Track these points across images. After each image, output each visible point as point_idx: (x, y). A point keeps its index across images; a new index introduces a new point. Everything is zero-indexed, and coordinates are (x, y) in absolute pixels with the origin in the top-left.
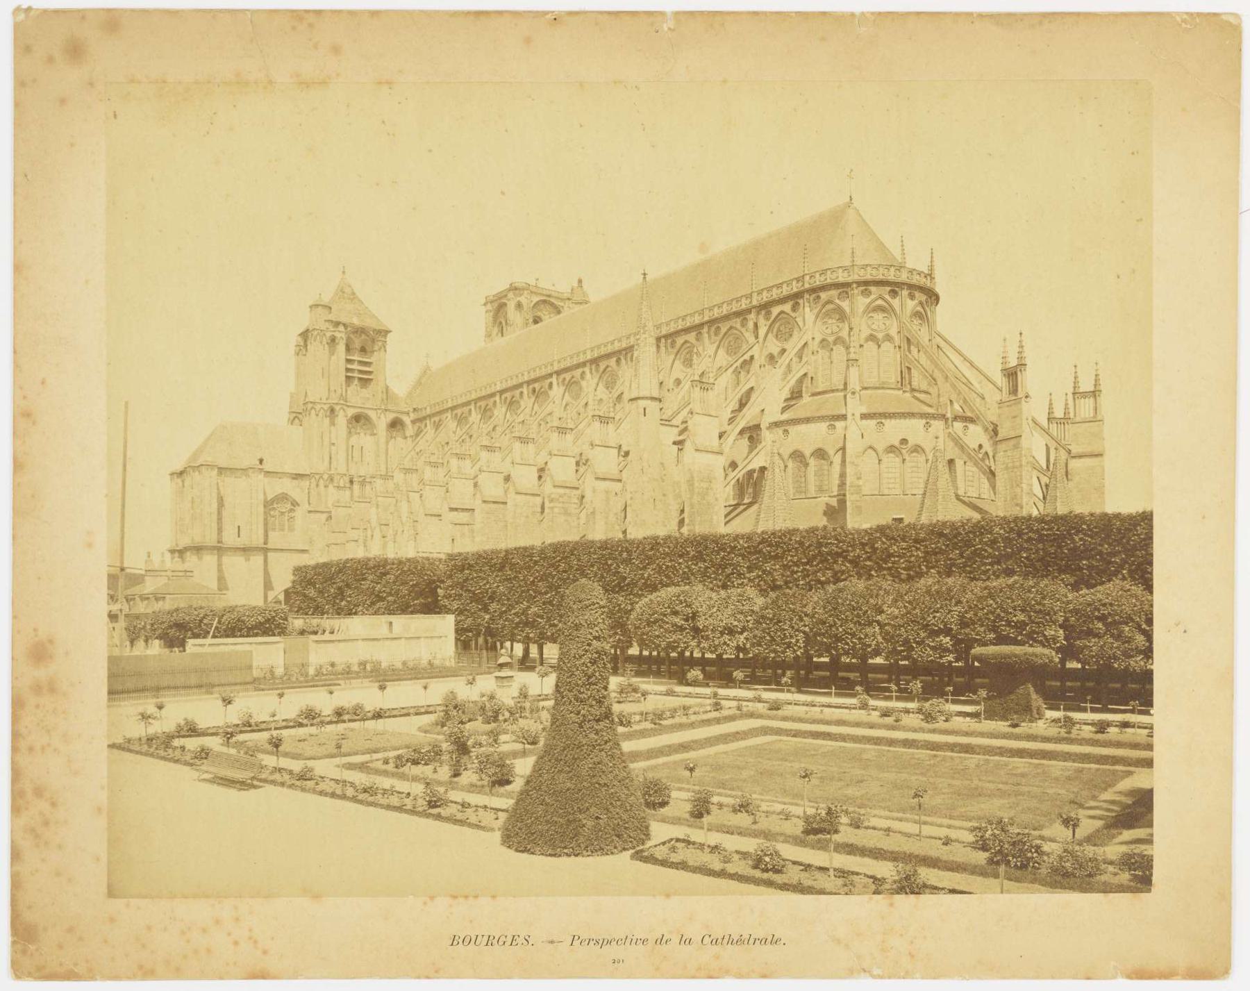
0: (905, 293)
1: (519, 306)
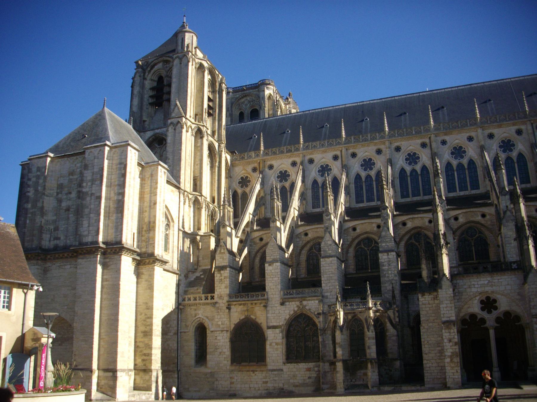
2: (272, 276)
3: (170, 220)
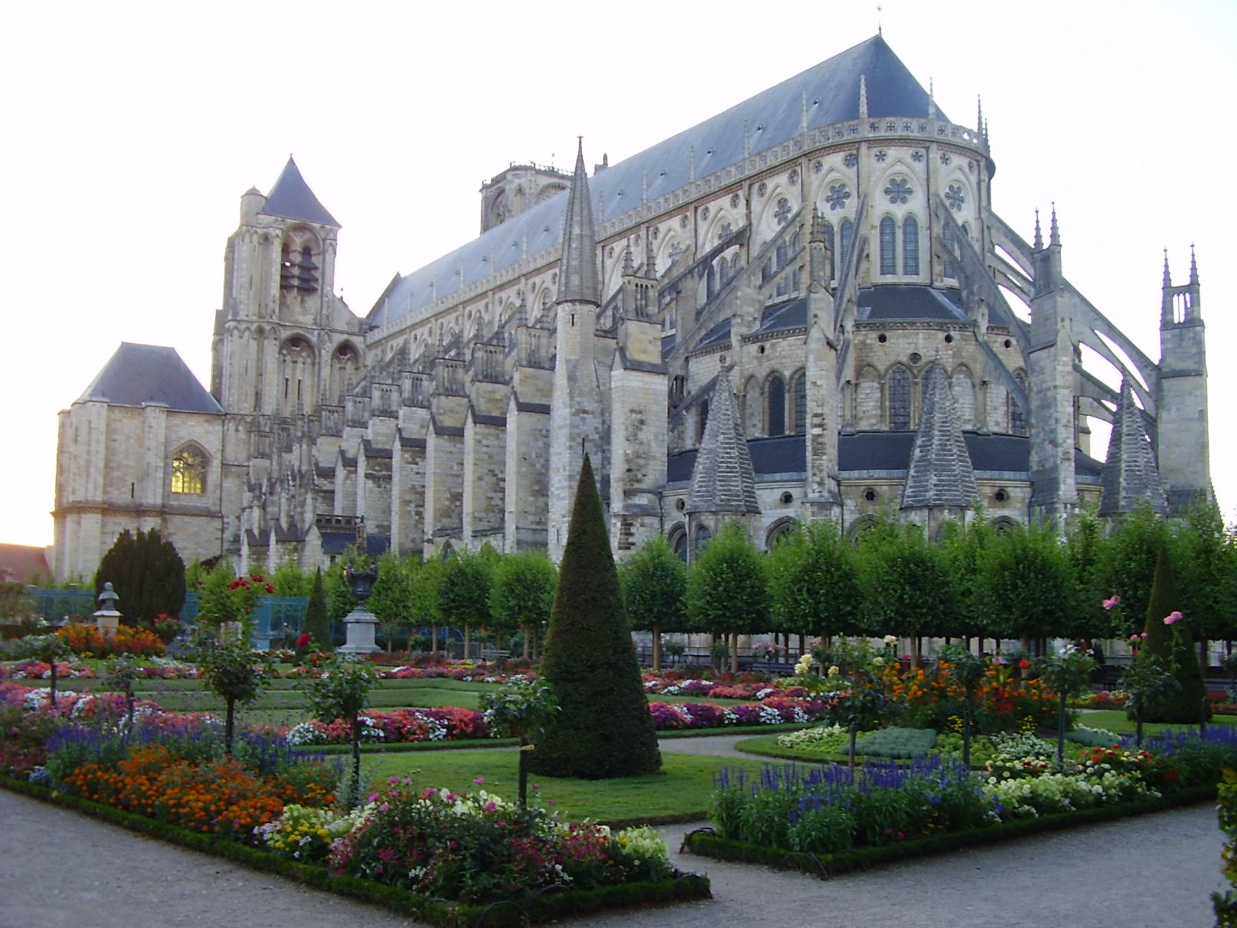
0: (935, 154)
1: (520, 190)
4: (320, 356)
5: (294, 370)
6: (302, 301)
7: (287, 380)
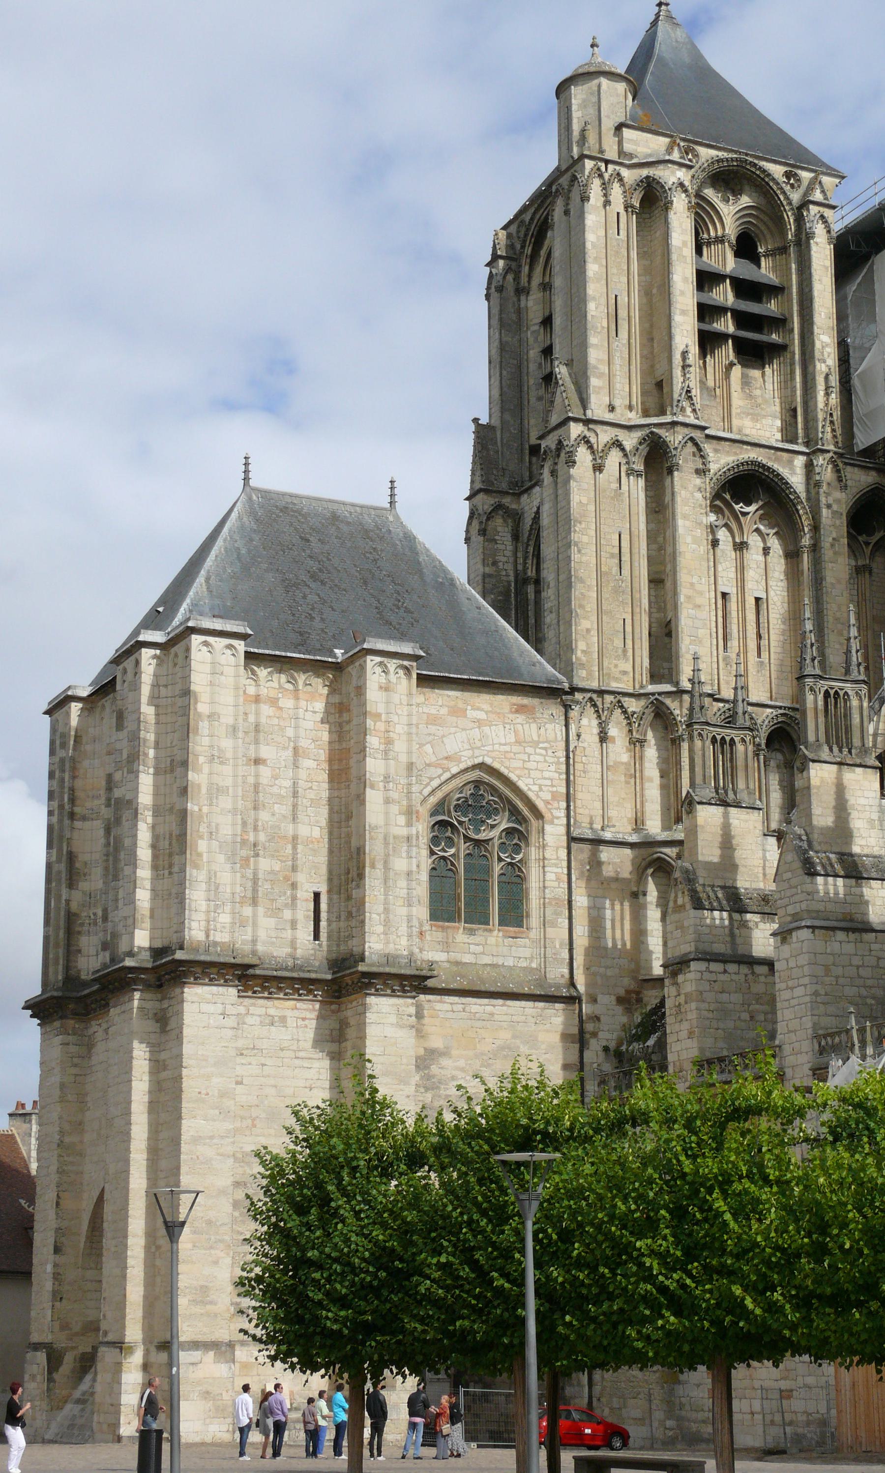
2: (790, 983)
3: (526, 811)
4: (816, 528)
5: (741, 569)
6: (746, 382)
7: (724, 595)
